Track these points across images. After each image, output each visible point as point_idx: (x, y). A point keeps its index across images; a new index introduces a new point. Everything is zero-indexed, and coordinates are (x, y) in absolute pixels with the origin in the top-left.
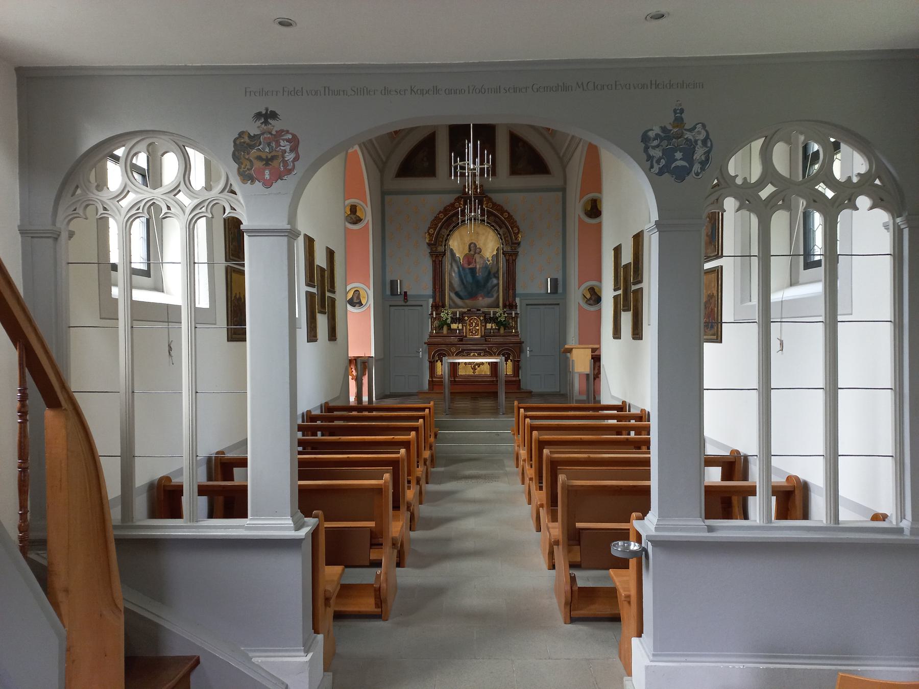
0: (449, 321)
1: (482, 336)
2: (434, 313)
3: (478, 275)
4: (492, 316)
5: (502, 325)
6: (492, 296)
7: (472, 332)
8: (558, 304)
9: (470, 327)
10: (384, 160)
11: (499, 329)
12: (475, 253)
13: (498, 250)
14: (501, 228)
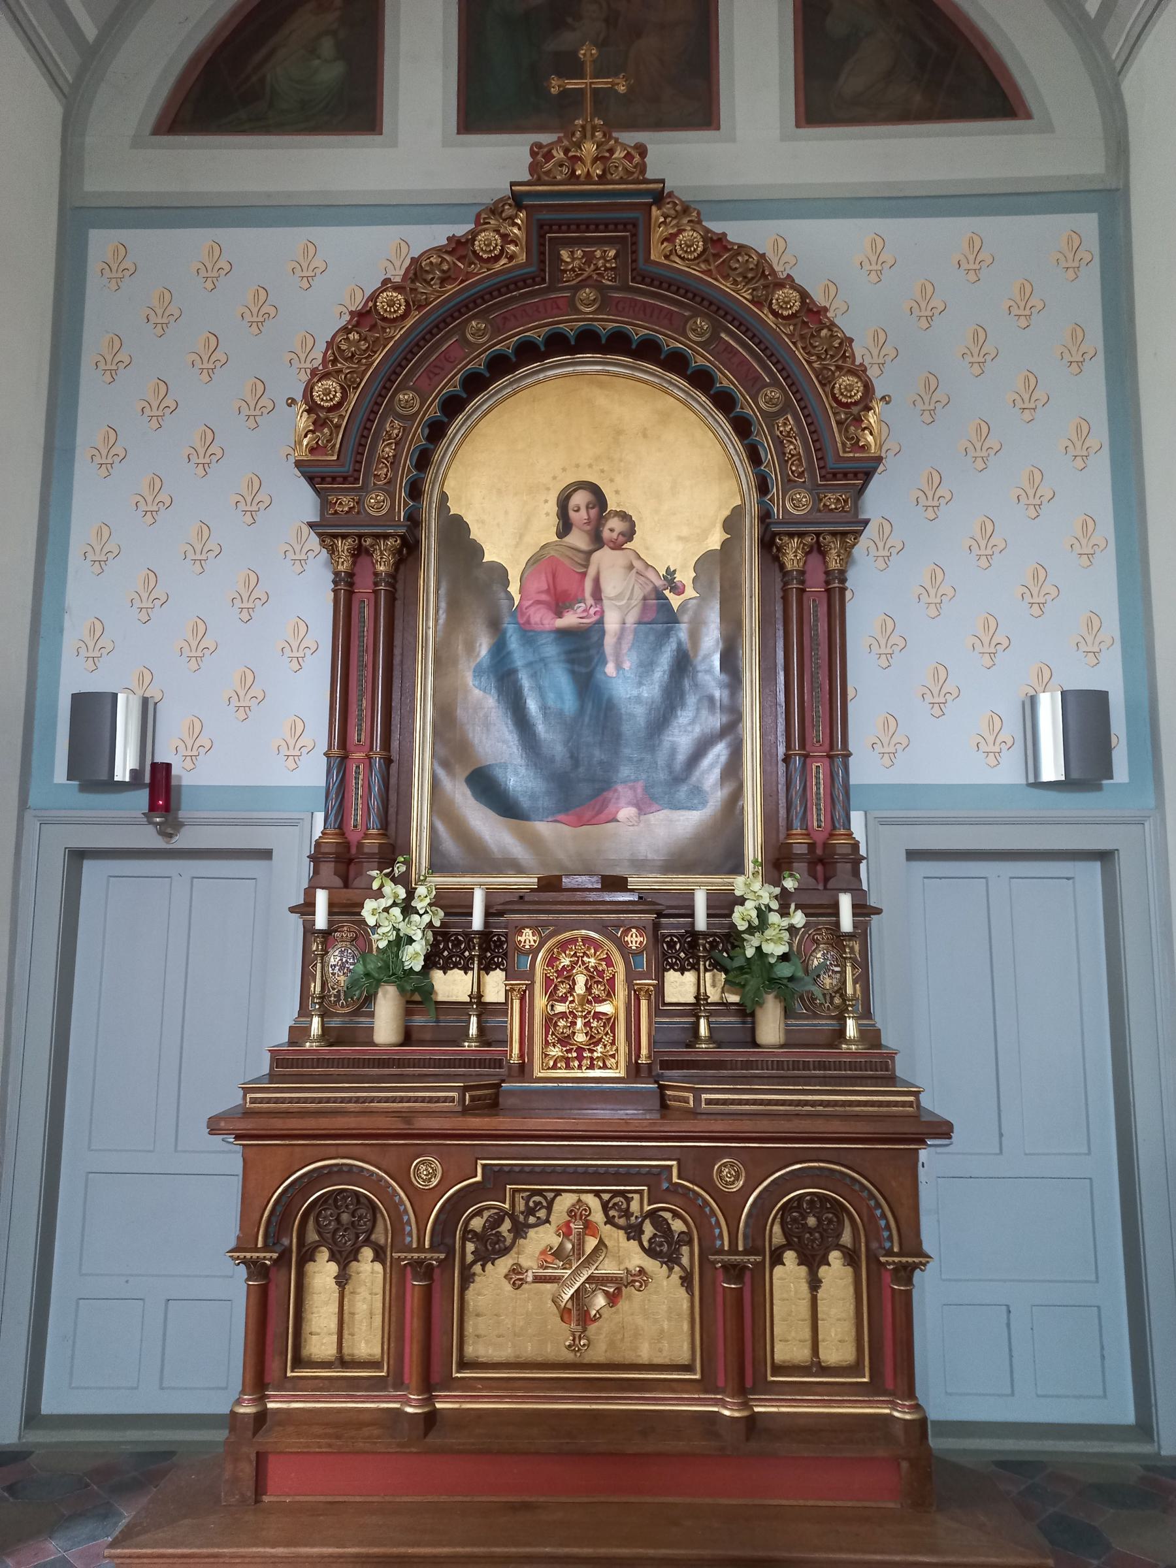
0: (414, 956)
1: (635, 1070)
2: (322, 898)
3: (610, 669)
4: (701, 923)
5: (773, 983)
6: (697, 796)
7: (565, 1040)
8: (1105, 857)
9: (553, 997)
10: (90, 32)
11: (747, 1013)
12: (598, 541)
13: (731, 524)
14: (754, 385)
